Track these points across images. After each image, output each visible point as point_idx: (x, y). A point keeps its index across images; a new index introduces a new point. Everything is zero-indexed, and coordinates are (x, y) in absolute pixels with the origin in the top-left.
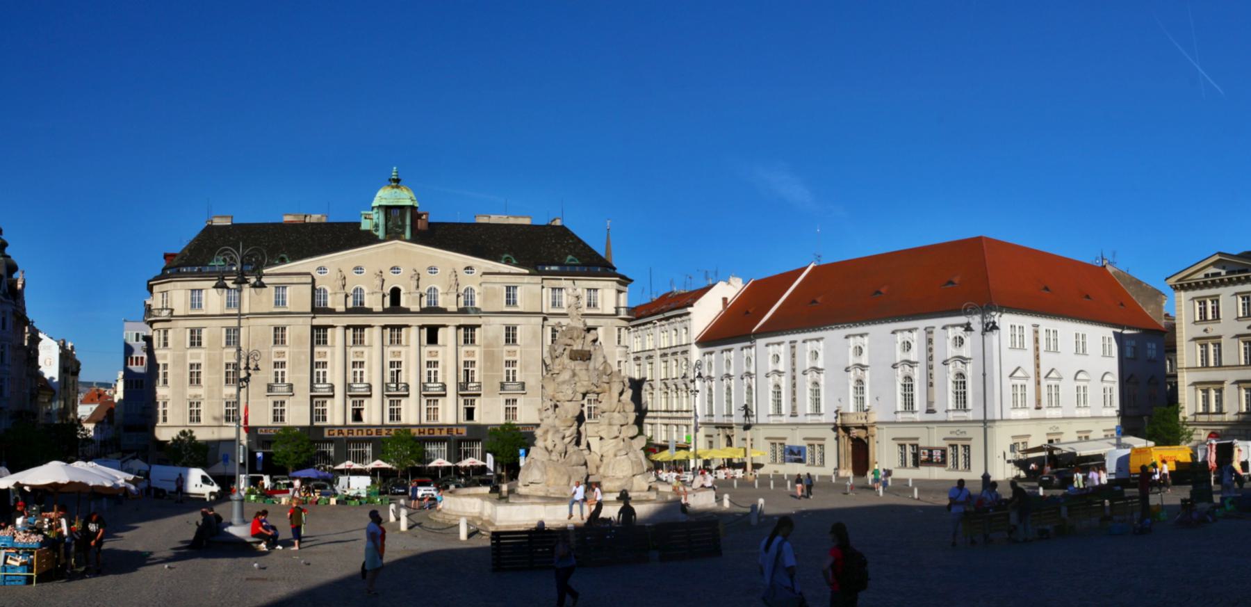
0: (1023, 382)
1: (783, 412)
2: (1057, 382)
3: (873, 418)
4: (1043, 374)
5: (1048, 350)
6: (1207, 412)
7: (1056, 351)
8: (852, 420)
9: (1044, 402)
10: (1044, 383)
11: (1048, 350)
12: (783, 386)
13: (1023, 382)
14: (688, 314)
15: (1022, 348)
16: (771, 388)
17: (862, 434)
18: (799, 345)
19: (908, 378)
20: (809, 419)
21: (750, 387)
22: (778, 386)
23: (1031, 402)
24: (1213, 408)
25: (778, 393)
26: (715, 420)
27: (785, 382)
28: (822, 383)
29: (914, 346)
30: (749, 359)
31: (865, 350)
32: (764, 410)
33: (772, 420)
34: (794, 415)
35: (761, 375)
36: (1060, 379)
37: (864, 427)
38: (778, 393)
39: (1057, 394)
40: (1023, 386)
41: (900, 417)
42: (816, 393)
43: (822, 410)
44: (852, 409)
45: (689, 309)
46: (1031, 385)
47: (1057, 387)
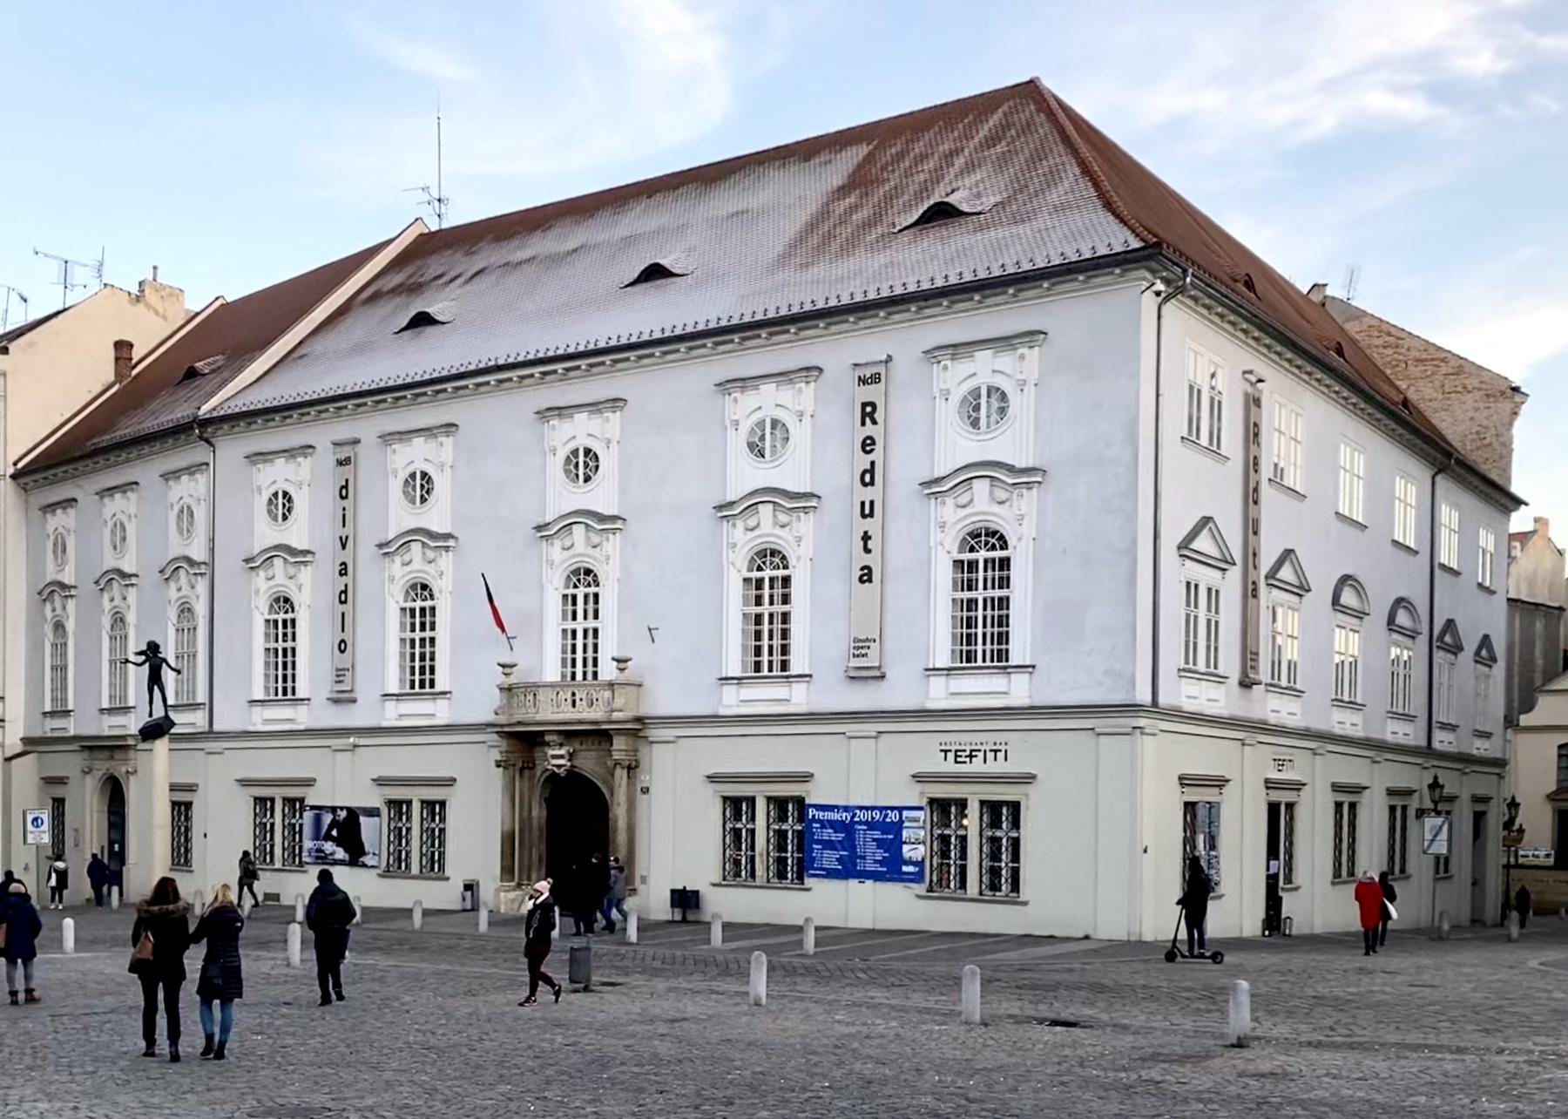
8: (550, 711)
16: (261, 612)
17: (588, 763)
18: (367, 455)
20: (392, 715)
21: (186, 610)
25: (283, 627)
26: (72, 727)
27: (311, 592)
30: (187, 513)
32: (238, 692)
33: (259, 719)
34: (343, 698)
35: (228, 565)
37: (599, 736)
38: (283, 627)
41: (732, 701)
42: (421, 618)
44: (552, 672)
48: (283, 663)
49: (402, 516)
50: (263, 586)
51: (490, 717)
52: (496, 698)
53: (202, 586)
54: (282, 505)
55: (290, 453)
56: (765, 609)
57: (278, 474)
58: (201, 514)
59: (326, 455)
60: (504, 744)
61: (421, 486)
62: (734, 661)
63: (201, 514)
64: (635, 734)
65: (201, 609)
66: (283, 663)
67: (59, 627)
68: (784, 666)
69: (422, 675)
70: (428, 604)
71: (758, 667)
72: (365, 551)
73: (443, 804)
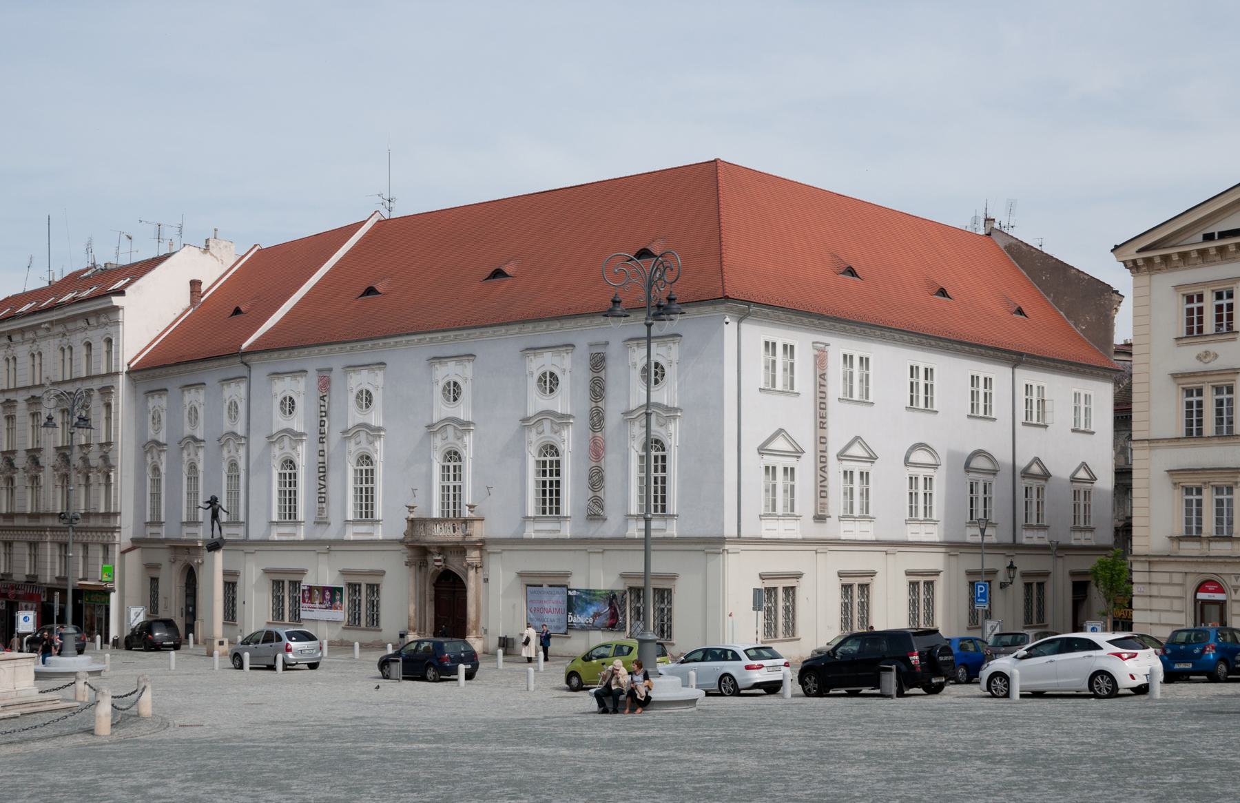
0: (790, 462)
1: (301, 516)
2: (865, 467)
3: (478, 532)
4: (833, 450)
5: (847, 398)
6: (1192, 534)
7: (865, 401)
9: (836, 504)
10: (835, 469)
11: (847, 398)
12: (301, 462)
13: (790, 462)
14: (116, 309)
15: (790, 390)
17: (454, 565)
18: (335, 377)
19: (552, 449)
21: (233, 465)
22: (290, 463)
23: (805, 503)
24: (1209, 527)
28: (379, 458)
29: (564, 381)
30: (234, 407)
31: (466, 389)
32: (262, 512)
34: (322, 522)
35: (258, 442)
36: (872, 459)
37: (460, 549)
38: (289, 479)
39: (866, 494)
40: (790, 472)
42: (366, 476)
43: (378, 514)
45: (116, 301)
46: (805, 469)
47: (864, 476)
48: (289, 500)
49: (355, 416)
50: (277, 453)
51: (401, 536)
52: (404, 526)
53: (242, 451)
54: (289, 405)
55: (294, 373)
56: (548, 478)
57: (284, 387)
58: (242, 407)
59: (313, 377)
60: (410, 552)
61: (366, 399)
62: (532, 509)
63: (242, 407)
64: (480, 548)
65: (242, 465)
66: (289, 500)
67: (156, 469)
68: (558, 511)
69: (366, 511)
70: (369, 467)
71: (544, 512)
72: (334, 436)
73: (378, 586)
